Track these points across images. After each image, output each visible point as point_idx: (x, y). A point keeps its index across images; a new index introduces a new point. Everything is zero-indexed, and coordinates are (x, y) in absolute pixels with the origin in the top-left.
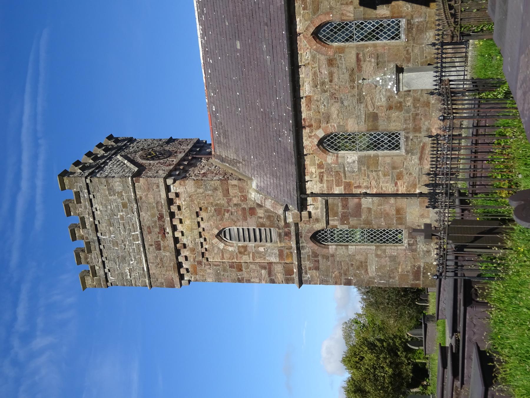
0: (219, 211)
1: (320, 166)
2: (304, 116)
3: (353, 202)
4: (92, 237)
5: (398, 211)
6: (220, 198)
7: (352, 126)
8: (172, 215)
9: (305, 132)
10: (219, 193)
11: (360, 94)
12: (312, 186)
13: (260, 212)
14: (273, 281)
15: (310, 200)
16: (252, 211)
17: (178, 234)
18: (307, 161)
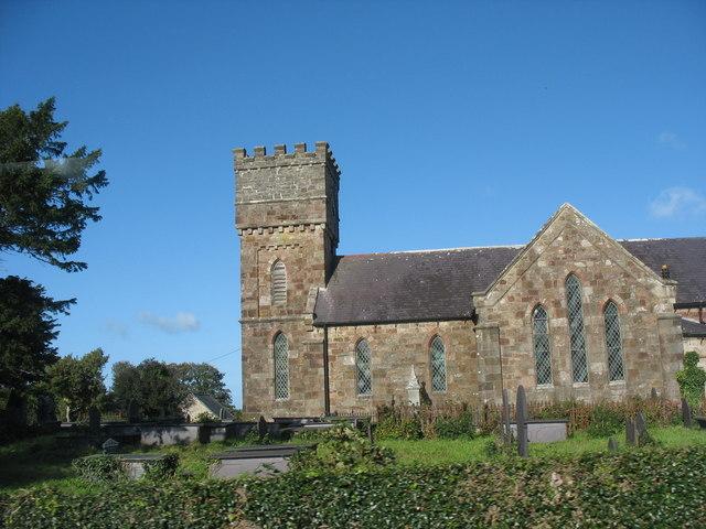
0: (300, 262)
1: (347, 339)
2: (383, 326)
3: (321, 362)
4: (277, 162)
5: (315, 393)
6: (311, 262)
7: (375, 361)
11: (398, 365)
12: (332, 330)
13: (299, 293)
14: (243, 301)
15: (322, 331)
16: (300, 287)
17: (280, 229)
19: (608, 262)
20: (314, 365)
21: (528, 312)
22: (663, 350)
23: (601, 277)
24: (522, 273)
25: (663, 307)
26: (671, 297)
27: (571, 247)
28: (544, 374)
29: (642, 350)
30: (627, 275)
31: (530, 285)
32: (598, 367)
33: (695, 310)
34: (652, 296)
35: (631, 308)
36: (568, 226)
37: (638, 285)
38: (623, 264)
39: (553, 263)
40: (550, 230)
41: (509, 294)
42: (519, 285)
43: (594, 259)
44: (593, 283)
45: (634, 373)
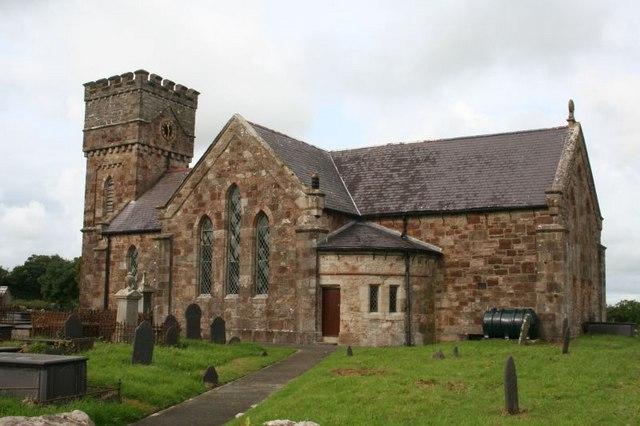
0: (122, 178)
3: (104, 266)
4: (111, 91)
6: (128, 178)
8: (120, 147)
9: (138, 237)
10: (130, 179)
17: (110, 150)
18: (126, 238)
19: (264, 173)
20: (100, 269)
21: (197, 223)
23: (255, 188)
24: (194, 187)
26: (313, 208)
27: (235, 159)
28: (206, 285)
29: (283, 264)
30: (277, 186)
32: (245, 280)
33: (400, 222)
34: (297, 207)
35: (277, 220)
36: (234, 137)
37: (286, 195)
38: (274, 174)
39: (220, 176)
40: (220, 142)
41: (184, 206)
42: (192, 197)
43: (251, 170)
44: (249, 195)
45: (275, 287)
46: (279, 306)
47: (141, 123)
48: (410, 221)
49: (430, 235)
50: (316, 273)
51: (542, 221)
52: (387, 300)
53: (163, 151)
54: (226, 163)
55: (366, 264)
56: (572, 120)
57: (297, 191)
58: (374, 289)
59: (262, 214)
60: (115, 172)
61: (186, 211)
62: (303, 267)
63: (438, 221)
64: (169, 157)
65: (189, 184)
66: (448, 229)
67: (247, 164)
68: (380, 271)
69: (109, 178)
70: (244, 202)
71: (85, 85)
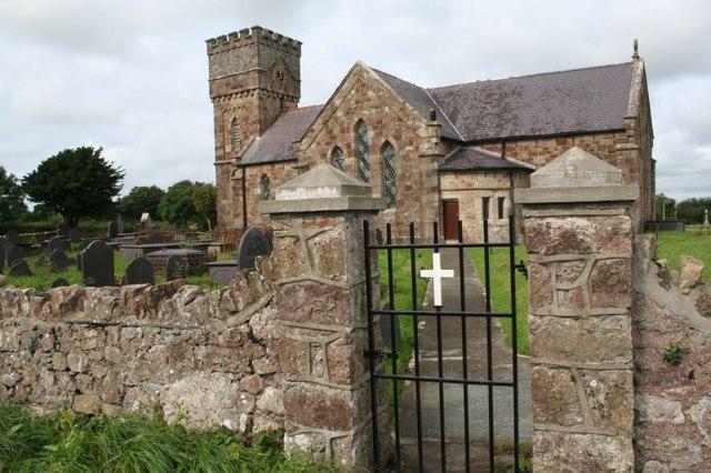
0: (246, 119)
3: (241, 192)
4: (231, 46)
6: (252, 118)
8: (242, 92)
12: (248, 171)
18: (258, 168)
19: (387, 109)
21: (330, 153)
22: (422, 184)
23: (380, 122)
24: (325, 123)
25: (426, 146)
29: (408, 183)
31: (330, 132)
33: (499, 146)
34: (418, 136)
35: (401, 148)
37: (408, 127)
38: (397, 110)
39: (348, 113)
40: (346, 85)
42: (324, 132)
44: (375, 128)
45: (402, 203)
46: (407, 218)
47: (260, 72)
48: (508, 145)
49: (526, 156)
50: (438, 190)
51: (620, 141)
52: (497, 209)
53: (278, 94)
54: (353, 102)
55: (479, 181)
56: (636, 57)
57: (417, 123)
58: (486, 201)
59: (387, 144)
60: (239, 114)
61: (319, 144)
62: (427, 185)
63: (532, 144)
64: (282, 99)
65: (320, 121)
66: (540, 150)
67: (371, 103)
68: (491, 186)
69: (235, 119)
70: (371, 134)
71: (208, 41)
